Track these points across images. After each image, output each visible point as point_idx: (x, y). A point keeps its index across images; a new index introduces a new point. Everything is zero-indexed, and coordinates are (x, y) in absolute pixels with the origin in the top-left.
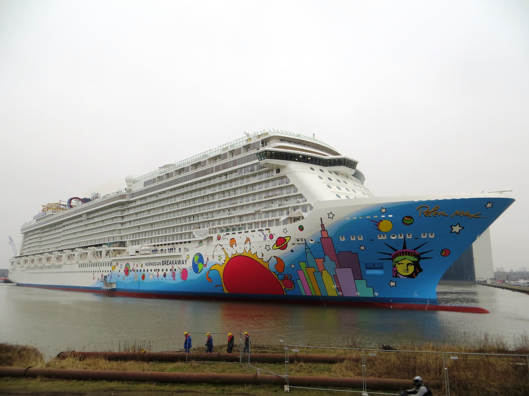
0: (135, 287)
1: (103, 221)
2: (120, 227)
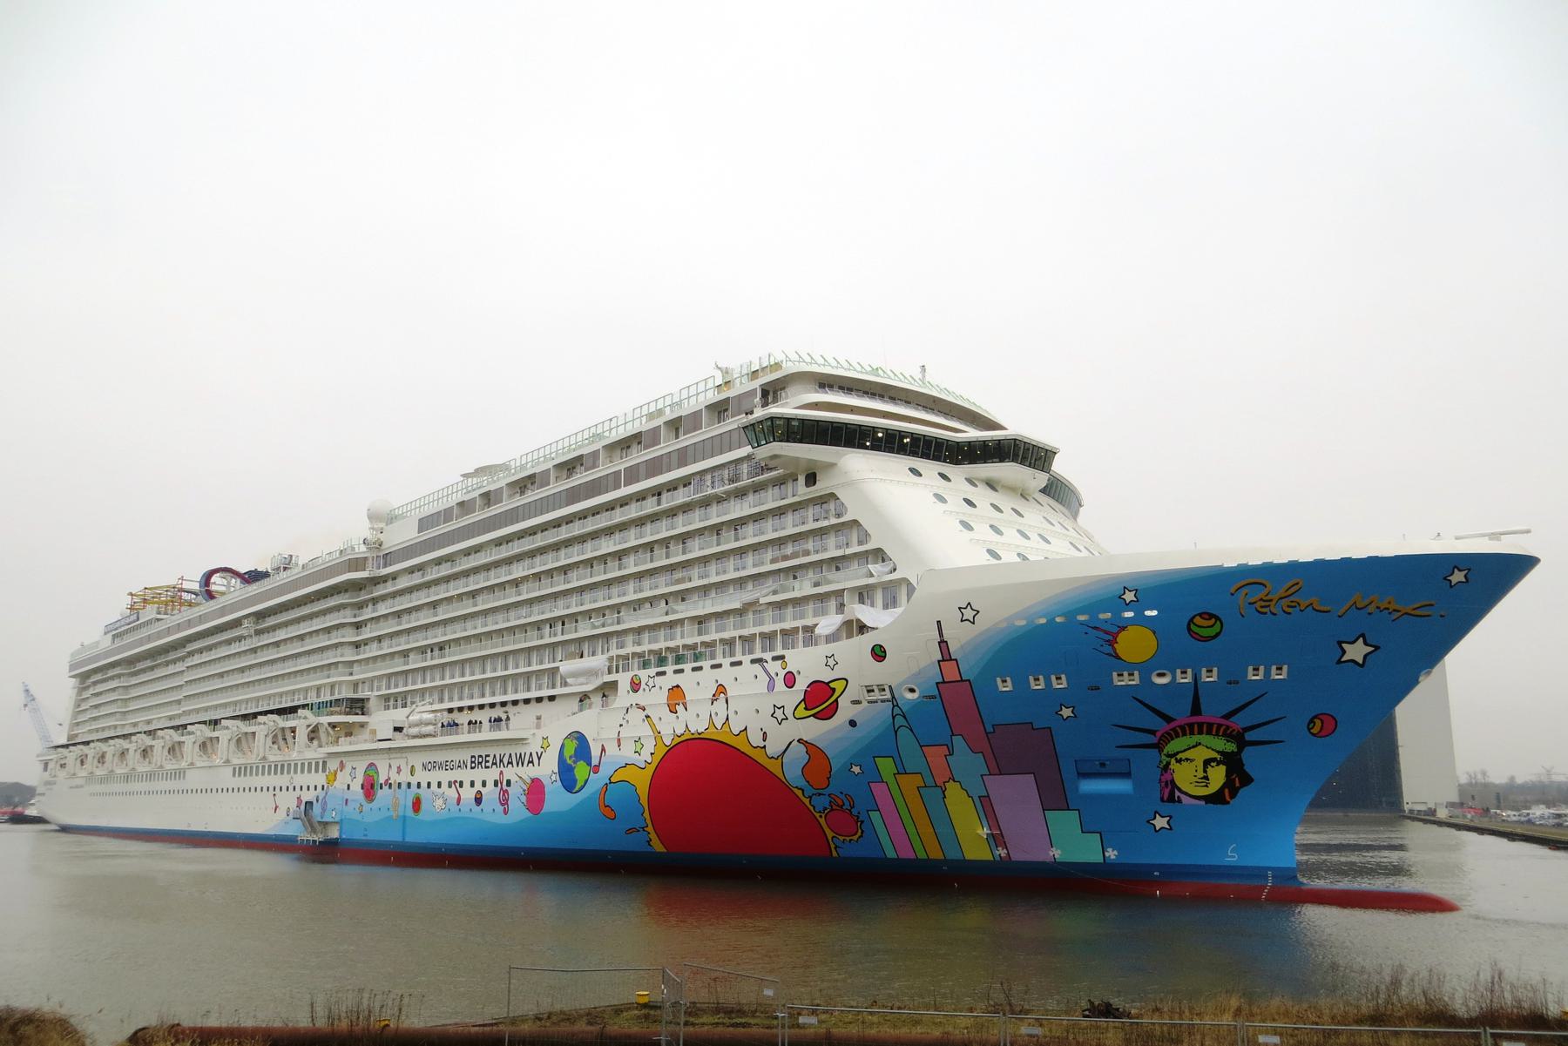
0: (392, 835)
1: (301, 637)
2: (349, 655)
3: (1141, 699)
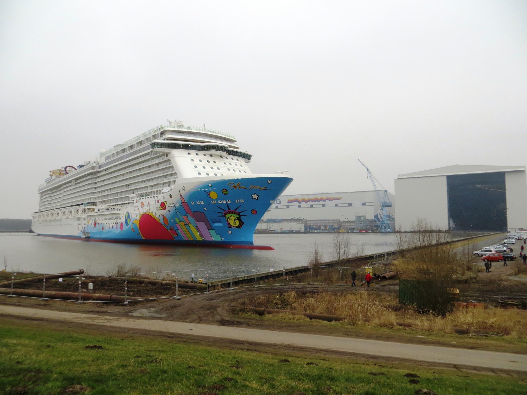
0: (98, 236)
1: (84, 186)
3: (218, 206)
